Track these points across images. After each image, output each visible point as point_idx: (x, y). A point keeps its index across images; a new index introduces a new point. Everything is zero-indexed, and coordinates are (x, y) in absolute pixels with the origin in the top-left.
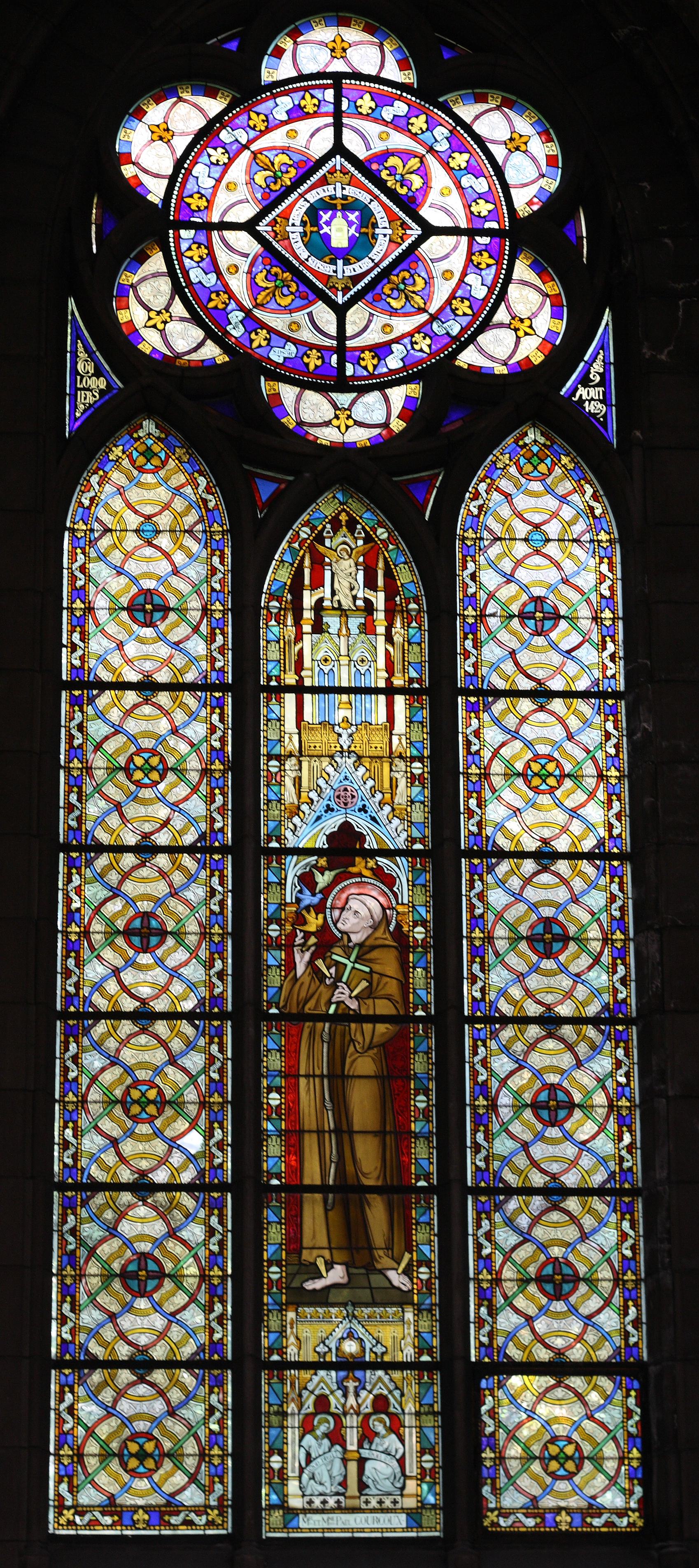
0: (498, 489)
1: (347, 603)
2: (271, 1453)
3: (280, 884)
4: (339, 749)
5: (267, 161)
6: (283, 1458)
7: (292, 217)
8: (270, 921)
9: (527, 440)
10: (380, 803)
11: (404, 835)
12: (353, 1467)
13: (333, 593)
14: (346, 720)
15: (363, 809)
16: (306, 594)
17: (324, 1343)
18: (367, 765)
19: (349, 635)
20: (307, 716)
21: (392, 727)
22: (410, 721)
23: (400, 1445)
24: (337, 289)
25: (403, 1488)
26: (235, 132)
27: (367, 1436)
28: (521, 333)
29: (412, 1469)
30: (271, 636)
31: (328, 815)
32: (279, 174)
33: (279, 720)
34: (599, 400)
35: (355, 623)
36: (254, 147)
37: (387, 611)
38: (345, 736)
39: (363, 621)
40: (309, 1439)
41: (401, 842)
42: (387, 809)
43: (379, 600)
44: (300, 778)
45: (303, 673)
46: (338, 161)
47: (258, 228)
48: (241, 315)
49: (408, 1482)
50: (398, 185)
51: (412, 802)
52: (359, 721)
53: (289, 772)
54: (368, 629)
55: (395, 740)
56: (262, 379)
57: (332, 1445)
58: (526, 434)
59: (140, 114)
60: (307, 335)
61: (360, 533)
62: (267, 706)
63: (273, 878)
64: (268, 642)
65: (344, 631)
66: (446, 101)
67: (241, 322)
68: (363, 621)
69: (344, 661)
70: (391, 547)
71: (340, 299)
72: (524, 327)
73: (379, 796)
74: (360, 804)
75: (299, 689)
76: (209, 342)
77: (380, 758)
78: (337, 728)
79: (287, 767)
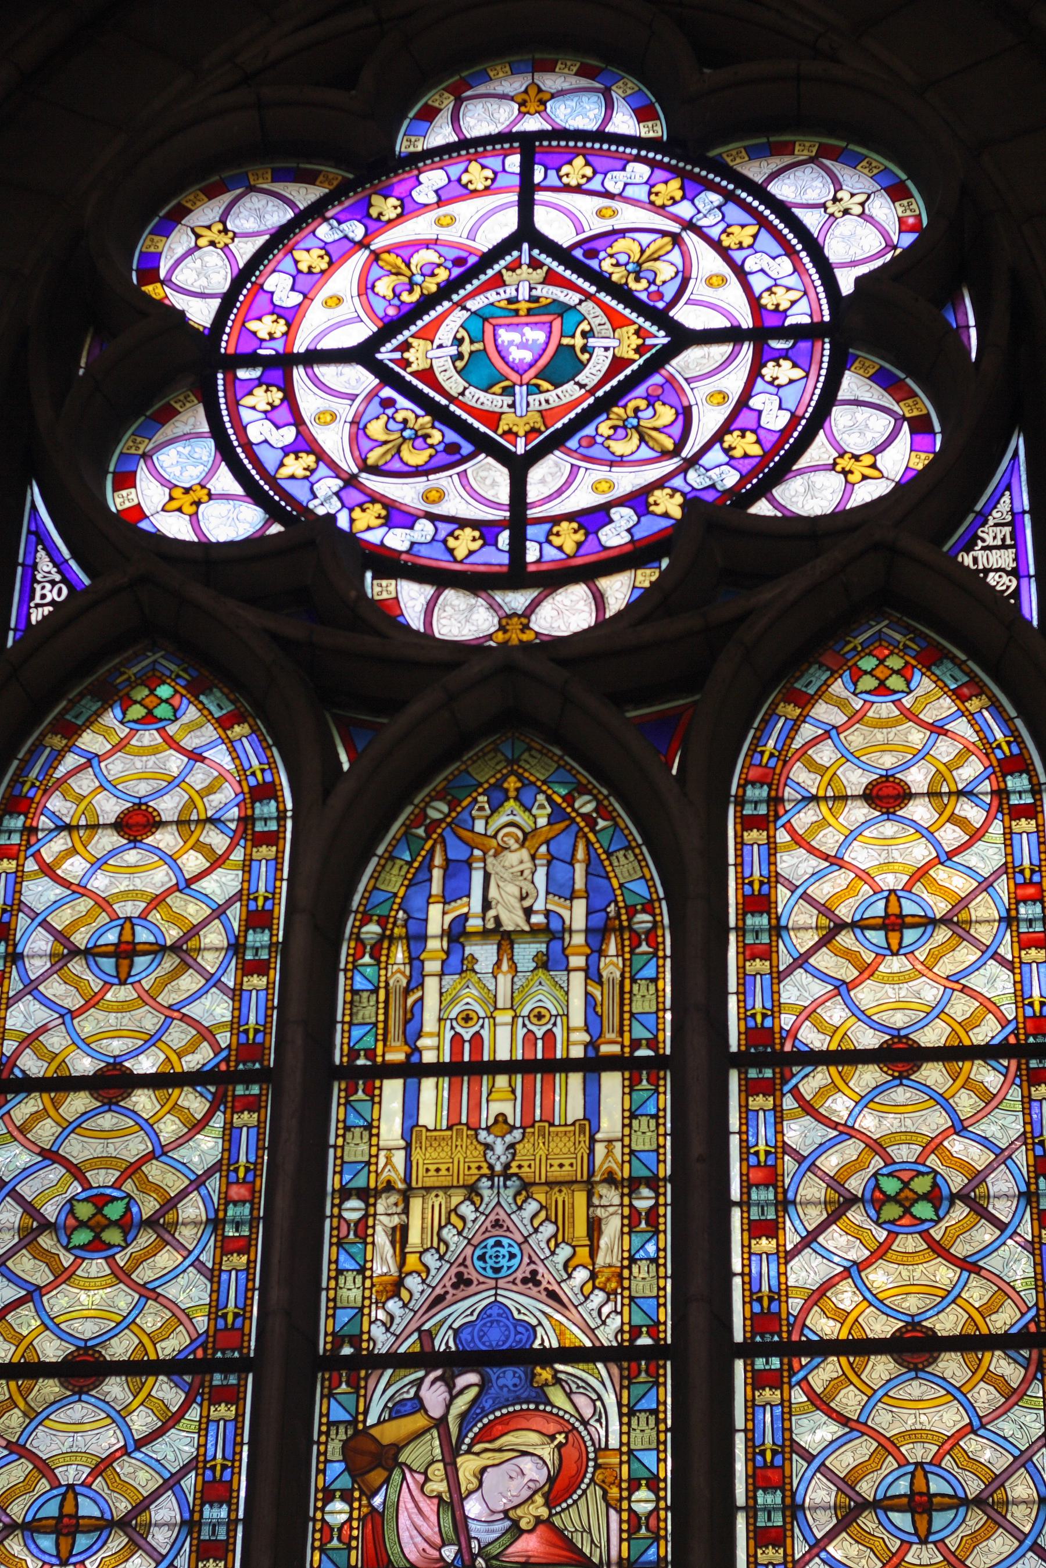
1: (512, 920)
4: (485, 1171)
5: (399, 261)
7: (439, 335)
10: (566, 1266)
11: (615, 1322)
13: (487, 905)
14: (500, 1118)
16: (435, 911)
18: (542, 1197)
19: (514, 968)
20: (427, 1118)
22: (632, 1115)
24: (516, 435)
26: (343, 226)
30: (360, 983)
33: (369, 1127)
35: (526, 953)
38: (499, 1148)
39: (543, 947)
41: (607, 1336)
42: (581, 1275)
44: (404, 1229)
47: (379, 356)
48: (336, 484)
50: (632, 276)
51: (632, 1260)
53: (385, 1219)
55: (600, 1149)
59: (179, 214)
60: (456, 505)
65: (505, 966)
66: (720, 155)
68: (543, 947)
70: (602, 824)
72: (859, 469)
73: (564, 1252)
74: (524, 1272)
78: (483, 1135)
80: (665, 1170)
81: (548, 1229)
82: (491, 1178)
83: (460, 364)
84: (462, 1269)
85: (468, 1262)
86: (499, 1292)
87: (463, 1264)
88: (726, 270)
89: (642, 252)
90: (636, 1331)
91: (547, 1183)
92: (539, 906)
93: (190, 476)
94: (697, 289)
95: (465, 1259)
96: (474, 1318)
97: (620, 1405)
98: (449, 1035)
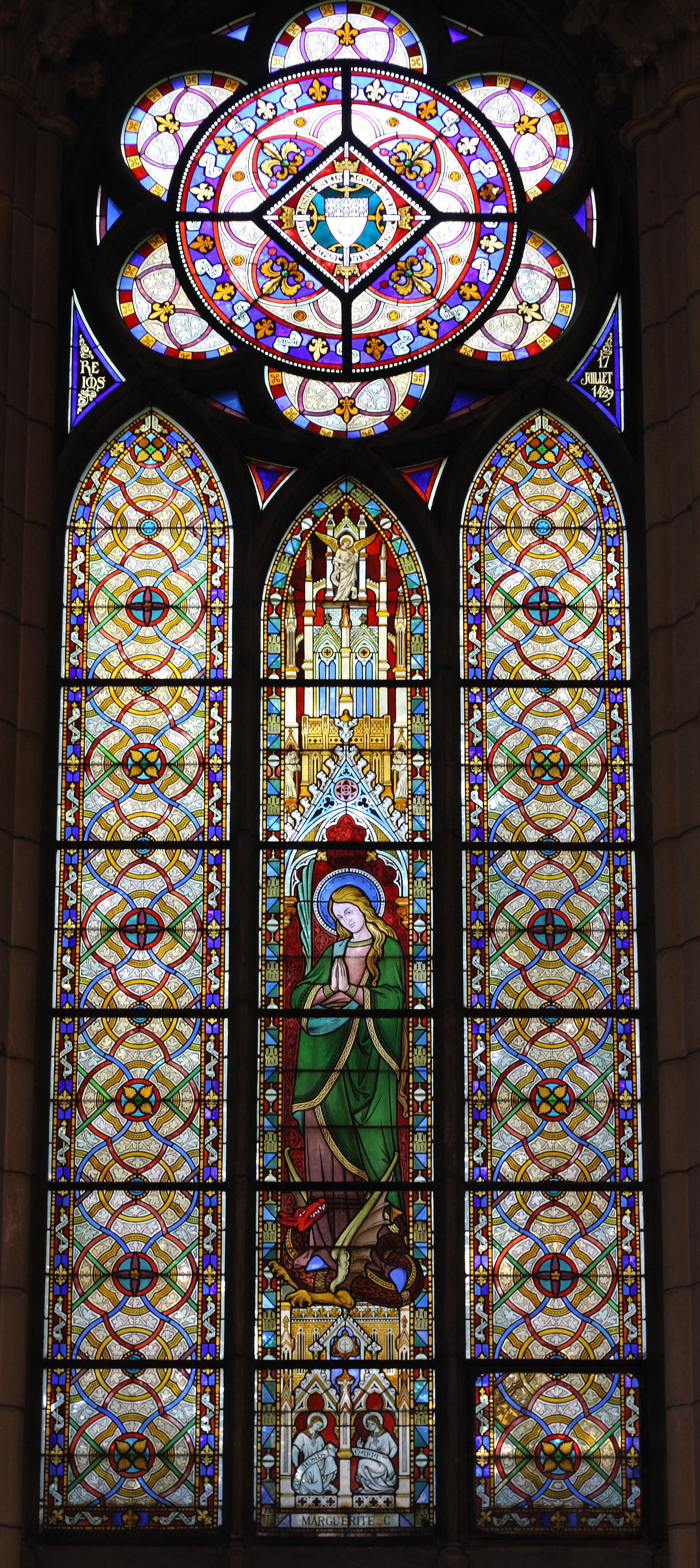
0: (504, 478)
2: (264, 1451)
3: (279, 878)
4: (339, 742)
6: (275, 1457)
8: (268, 916)
9: (534, 428)
11: (405, 829)
12: (345, 1465)
14: (345, 712)
15: (363, 803)
16: (308, 586)
17: (318, 1341)
19: (350, 626)
20: (308, 710)
21: (393, 720)
22: (412, 714)
23: (393, 1444)
25: (396, 1486)
27: (360, 1434)
28: (528, 319)
29: (405, 1469)
32: (286, 163)
33: (280, 714)
34: (608, 385)
36: (262, 136)
37: (388, 603)
38: (346, 729)
39: (365, 612)
40: (302, 1438)
42: (388, 802)
43: (382, 591)
45: (304, 666)
46: (347, 149)
47: (265, 217)
49: (401, 1482)
51: (413, 795)
52: (360, 715)
53: (289, 767)
54: (371, 620)
55: (396, 732)
56: (266, 368)
57: (326, 1444)
58: (533, 422)
59: (146, 105)
60: (312, 323)
61: (362, 523)
62: (268, 700)
63: (271, 872)
64: (269, 634)
67: (247, 312)
69: (346, 652)
71: (347, 287)
73: (379, 789)
74: (359, 799)
75: (300, 683)
76: (214, 332)
77: (381, 751)
79: (287, 761)
80: (428, 745)
81: (371, 776)
82: (342, 746)
83: (312, 229)
88: (460, 170)
89: (413, 153)
90: (415, 834)
91: (370, 750)
92: (362, 586)
93: (163, 295)
94: (444, 181)
97: (408, 873)
98: (318, 661)
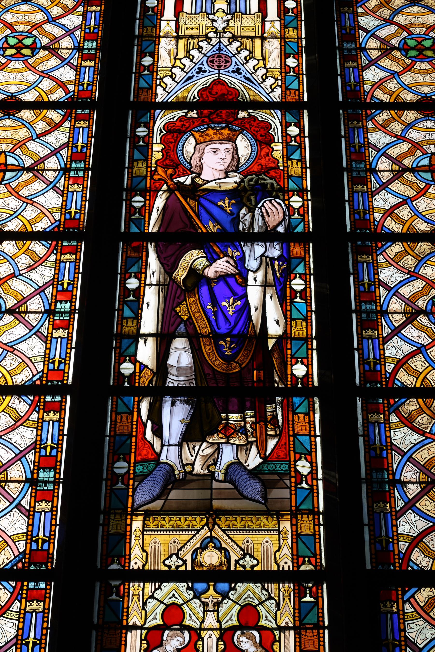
31: (200, 76)
84: (201, 66)
85: (205, 63)
86: (220, 75)
87: (202, 64)
95: (203, 62)
96: (207, 86)
